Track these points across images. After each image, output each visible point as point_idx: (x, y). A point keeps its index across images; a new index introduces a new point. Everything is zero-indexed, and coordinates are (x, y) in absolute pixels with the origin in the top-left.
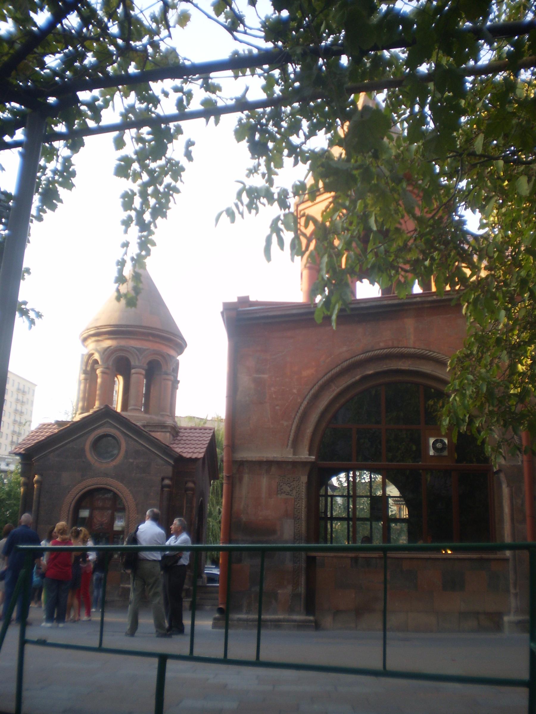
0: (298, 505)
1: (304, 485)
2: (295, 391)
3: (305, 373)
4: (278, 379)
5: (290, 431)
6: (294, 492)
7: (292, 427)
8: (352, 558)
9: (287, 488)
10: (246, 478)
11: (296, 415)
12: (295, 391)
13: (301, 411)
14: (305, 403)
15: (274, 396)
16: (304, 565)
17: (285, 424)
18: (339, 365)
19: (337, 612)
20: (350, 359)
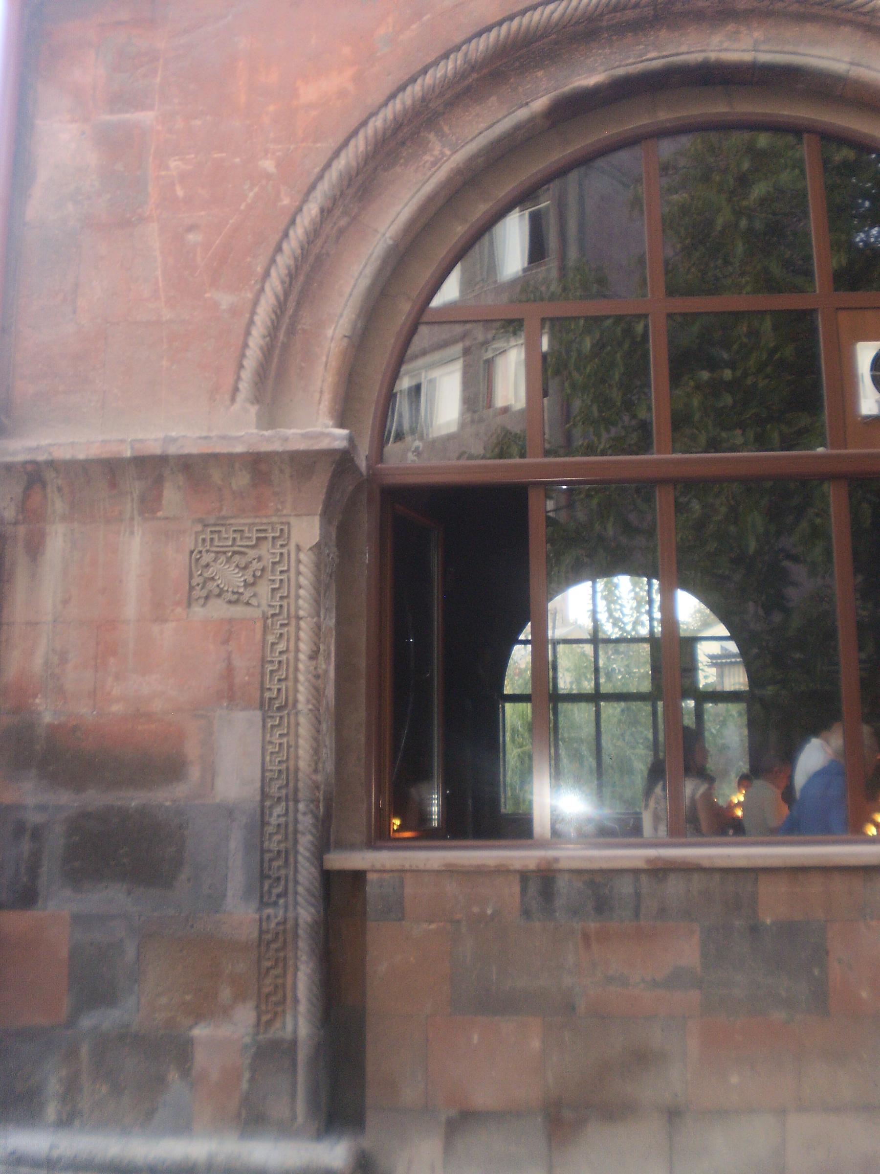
0: (282, 646)
1: (306, 557)
2: (268, 165)
3: (309, 93)
4: (198, 123)
5: (248, 333)
6: (264, 589)
7: (253, 313)
8: (524, 876)
9: (230, 576)
10: (57, 541)
11: (273, 261)
12: (268, 165)
13: (292, 245)
14: (312, 209)
15: (180, 192)
16: (306, 914)
17: (225, 300)
18: (457, 48)
19: (462, 1121)
20: (500, 23)
